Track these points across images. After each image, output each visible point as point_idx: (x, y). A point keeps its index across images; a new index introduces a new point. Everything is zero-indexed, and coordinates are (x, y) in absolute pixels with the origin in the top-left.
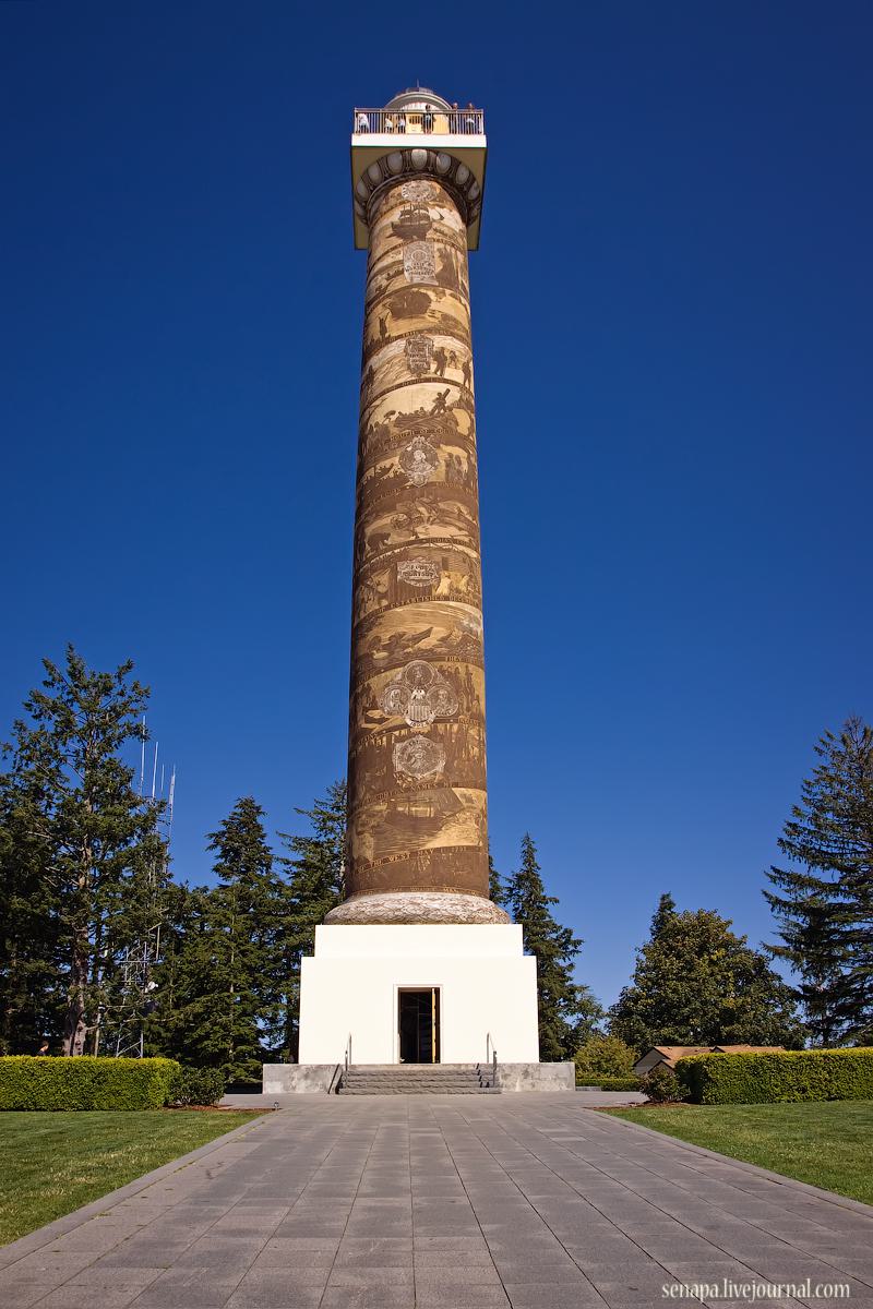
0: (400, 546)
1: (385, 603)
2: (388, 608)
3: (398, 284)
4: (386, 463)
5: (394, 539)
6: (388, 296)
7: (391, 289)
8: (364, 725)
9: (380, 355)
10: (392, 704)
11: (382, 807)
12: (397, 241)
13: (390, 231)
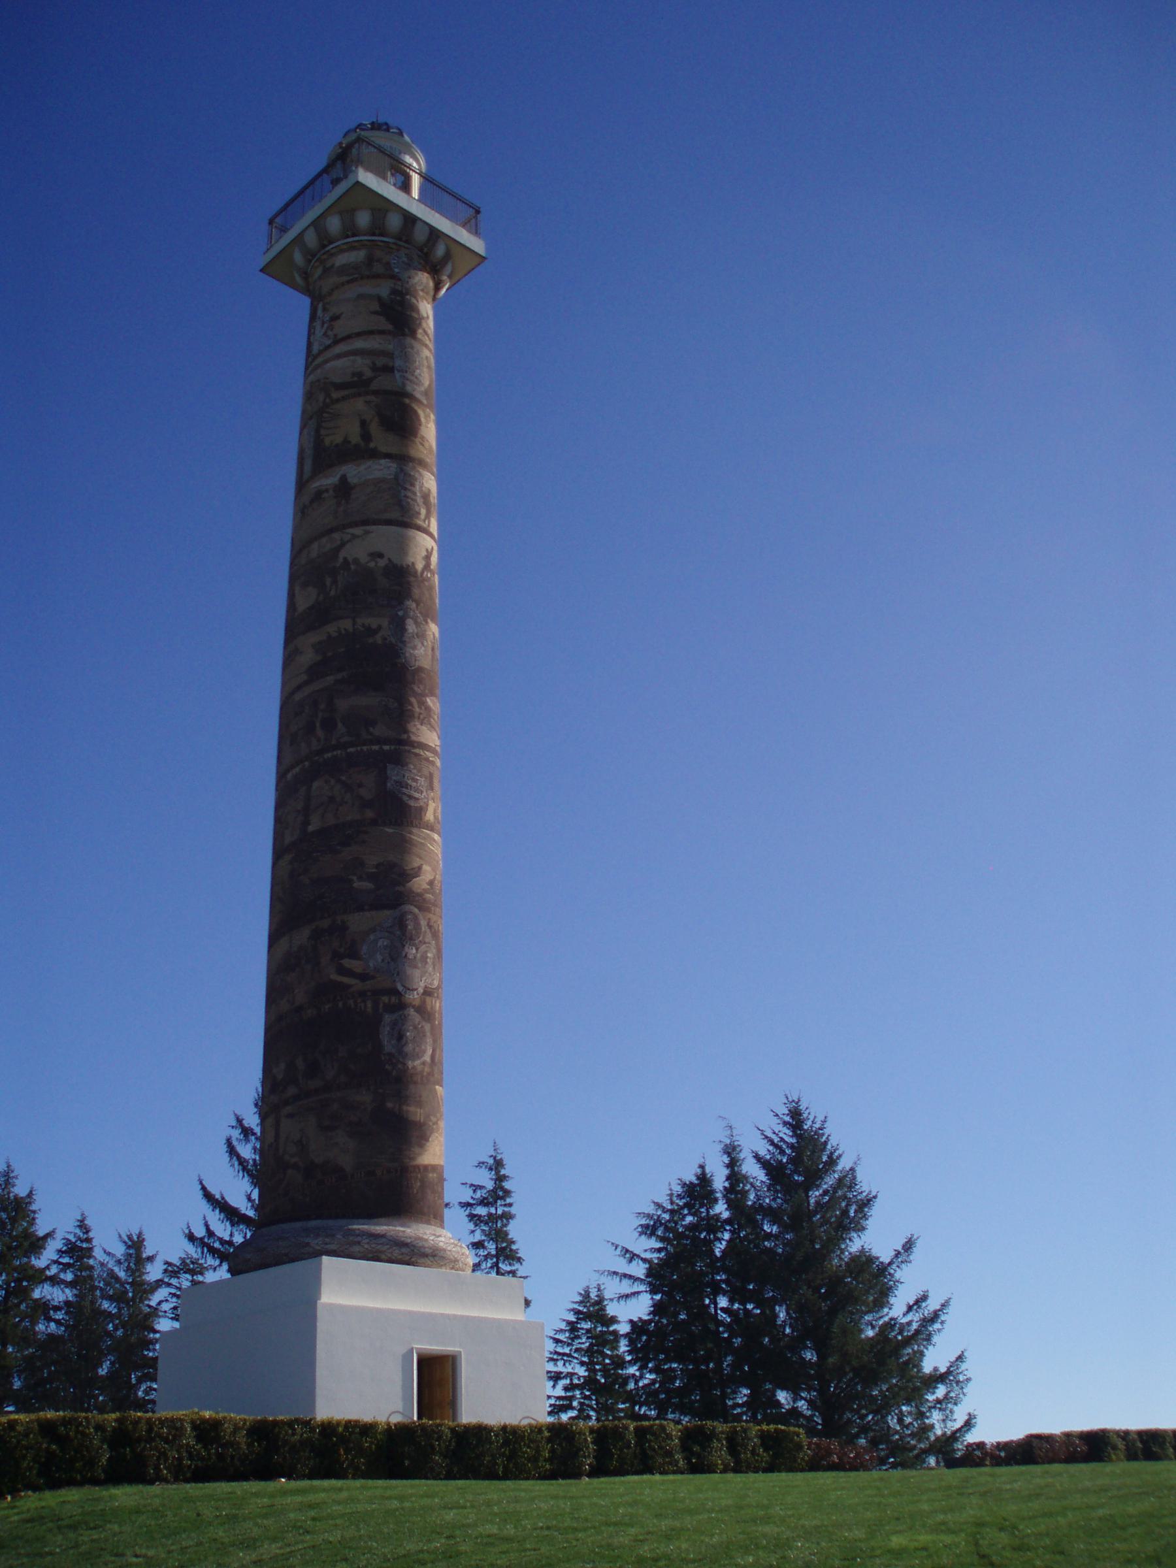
0: (387, 741)
1: (370, 814)
2: (374, 822)
3: (382, 382)
4: (373, 622)
5: (379, 731)
6: (376, 393)
7: (374, 386)
8: (335, 977)
9: (362, 468)
10: (379, 957)
11: (365, 1098)
12: (383, 323)
13: (375, 306)
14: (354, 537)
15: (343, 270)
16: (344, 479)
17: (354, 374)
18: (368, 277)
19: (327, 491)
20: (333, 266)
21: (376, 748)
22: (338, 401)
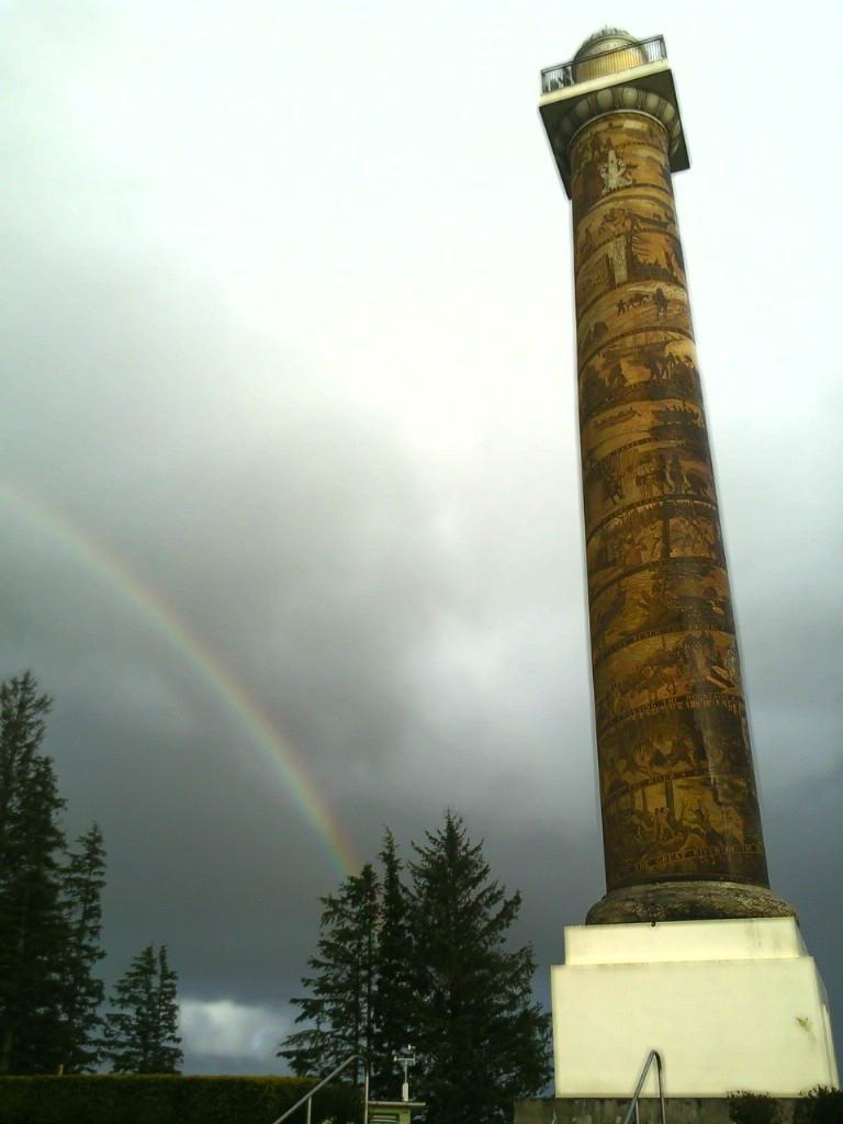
14: (675, 339)
15: (631, 132)
16: (659, 291)
17: (655, 215)
18: (652, 146)
19: (647, 296)
20: (621, 126)
21: (710, 505)
22: (645, 230)
